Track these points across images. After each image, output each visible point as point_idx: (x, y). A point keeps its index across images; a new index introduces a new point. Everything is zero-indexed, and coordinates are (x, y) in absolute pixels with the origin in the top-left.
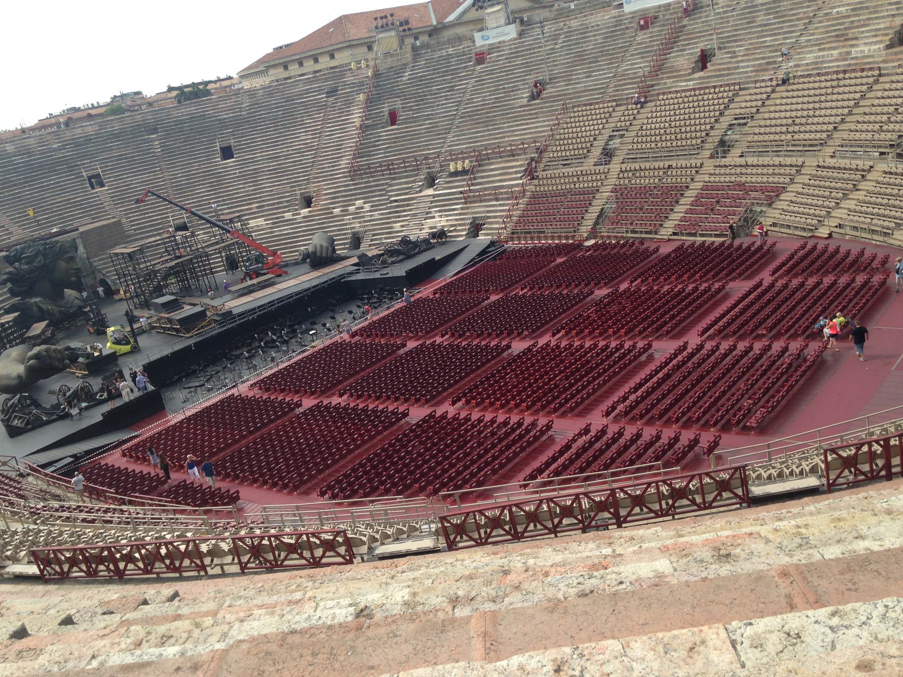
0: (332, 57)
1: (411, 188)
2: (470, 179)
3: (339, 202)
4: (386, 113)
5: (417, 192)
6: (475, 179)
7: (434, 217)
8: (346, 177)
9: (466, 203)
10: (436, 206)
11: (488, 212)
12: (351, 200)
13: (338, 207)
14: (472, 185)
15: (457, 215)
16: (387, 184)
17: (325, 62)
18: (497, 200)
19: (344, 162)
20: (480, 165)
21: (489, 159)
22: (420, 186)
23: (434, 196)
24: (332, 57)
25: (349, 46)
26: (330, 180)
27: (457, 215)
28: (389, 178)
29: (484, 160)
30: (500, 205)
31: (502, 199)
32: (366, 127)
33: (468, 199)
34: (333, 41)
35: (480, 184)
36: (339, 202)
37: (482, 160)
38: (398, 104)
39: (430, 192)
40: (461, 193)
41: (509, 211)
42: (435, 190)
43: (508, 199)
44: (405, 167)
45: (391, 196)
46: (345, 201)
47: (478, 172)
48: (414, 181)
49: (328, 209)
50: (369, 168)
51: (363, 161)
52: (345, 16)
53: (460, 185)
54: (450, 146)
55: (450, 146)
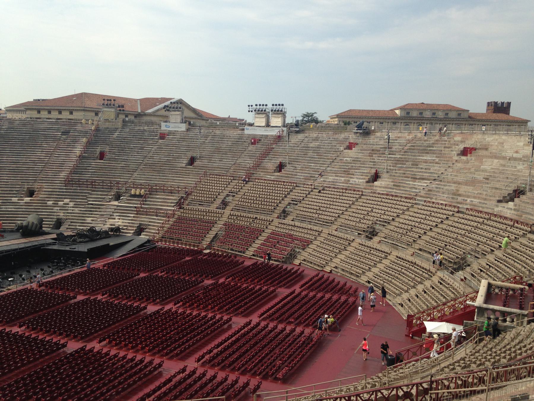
0: (71, 113)
1: (104, 198)
2: (143, 201)
3: (53, 198)
4: (98, 152)
5: (107, 202)
6: (146, 201)
7: (115, 219)
8: (62, 183)
9: (137, 214)
10: (117, 213)
11: (150, 222)
12: (62, 198)
13: (51, 201)
14: (144, 204)
15: (130, 220)
16: (88, 193)
17: (65, 115)
18: (157, 216)
19: (63, 175)
20: (150, 194)
21: (156, 192)
22: (110, 198)
23: (118, 206)
24: (71, 113)
25: (84, 110)
26: (50, 183)
27: (130, 220)
28: (91, 190)
29: (154, 192)
30: (158, 219)
31: (160, 216)
32: (83, 157)
33: (138, 212)
34: (75, 105)
35: (148, 205)
36: (53, 198)
37: (152, 192)
38: (107, 149)
39: (116, 203)
40: (135, 207)
41: (163, 224)
42: (119, 203)
43: (163, 217)
44: (103, 185)
45: (90, 201)
46: (57, 198)
47: (148, 197)
48: (107, 195)
49: (44, 200)
50: (79, 181)
51: (76, 176)
52: (85, 93)
53: (136, 203)
54: (134, 179)
55: (134, 179)
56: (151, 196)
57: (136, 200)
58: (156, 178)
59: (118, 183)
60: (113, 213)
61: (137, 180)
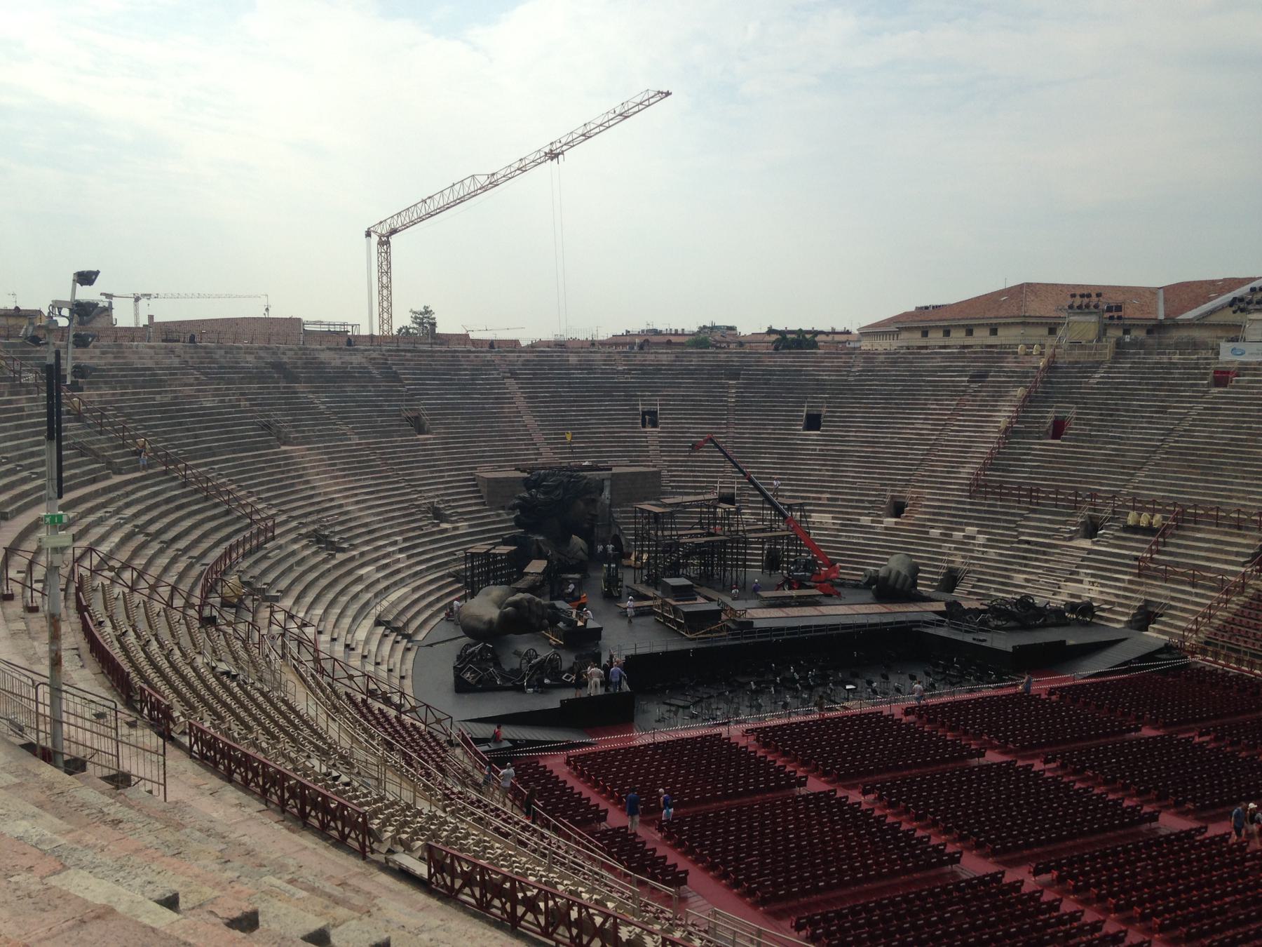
0: (994, 332)
1: (1057, 530)
2: (1157, 543)
3: (942, 521)
4: (1050, 421)
5: (1065, 539)
6: (1165, 544)
7: (1081, 582)
8: (963, 491)
9: (1139, 575)
10: (1088, 567)
11: (1173, 599)
12: (961, 523)
13: (939, 528)
14: (1158, 552)
15: (1119, 588)
16: (1021, 515)
17: (981, 337)
18: (1194, 585)
19: (966, 471)
20: (1178, 528)
21: (1196, 522)
22: (1071, 532)
23: (1090, 551)
24: (994, 332)
25: (1023, 324)
26: (939, 489)
27: (1119, 588)
28: (1028, 509)
29: (1189, 521)
30: (1197, 595)
31: (1203, 587)
32: (1013, 432)
33: (1144, 571)
34: (1002, 313)
35: (1171, 554)
36: (942, 521)
37: (1184, 521)
38: (1071, 412)
39: (1086, 544)
40: (1136, 558)
41: (1210, 607)
42: (1094, 543)
43: (1212, 589)
44: (1056, 499)
45: (1023, 534)
46: (951, 522)
47: (1173, 536)
48: (1064, 523)
49: (924, 526)
50: (1001, 487)
51: (995, 476)
52: (1028, 285)
53: (1138, 548)
54: (1137, 488)
55: (1137, 488)
56: (1182, 533)
57: (1137, 541)
58: (1196, 487)
59: (1094, 495)
60: (1078, 566)
61: (1143, 488)
